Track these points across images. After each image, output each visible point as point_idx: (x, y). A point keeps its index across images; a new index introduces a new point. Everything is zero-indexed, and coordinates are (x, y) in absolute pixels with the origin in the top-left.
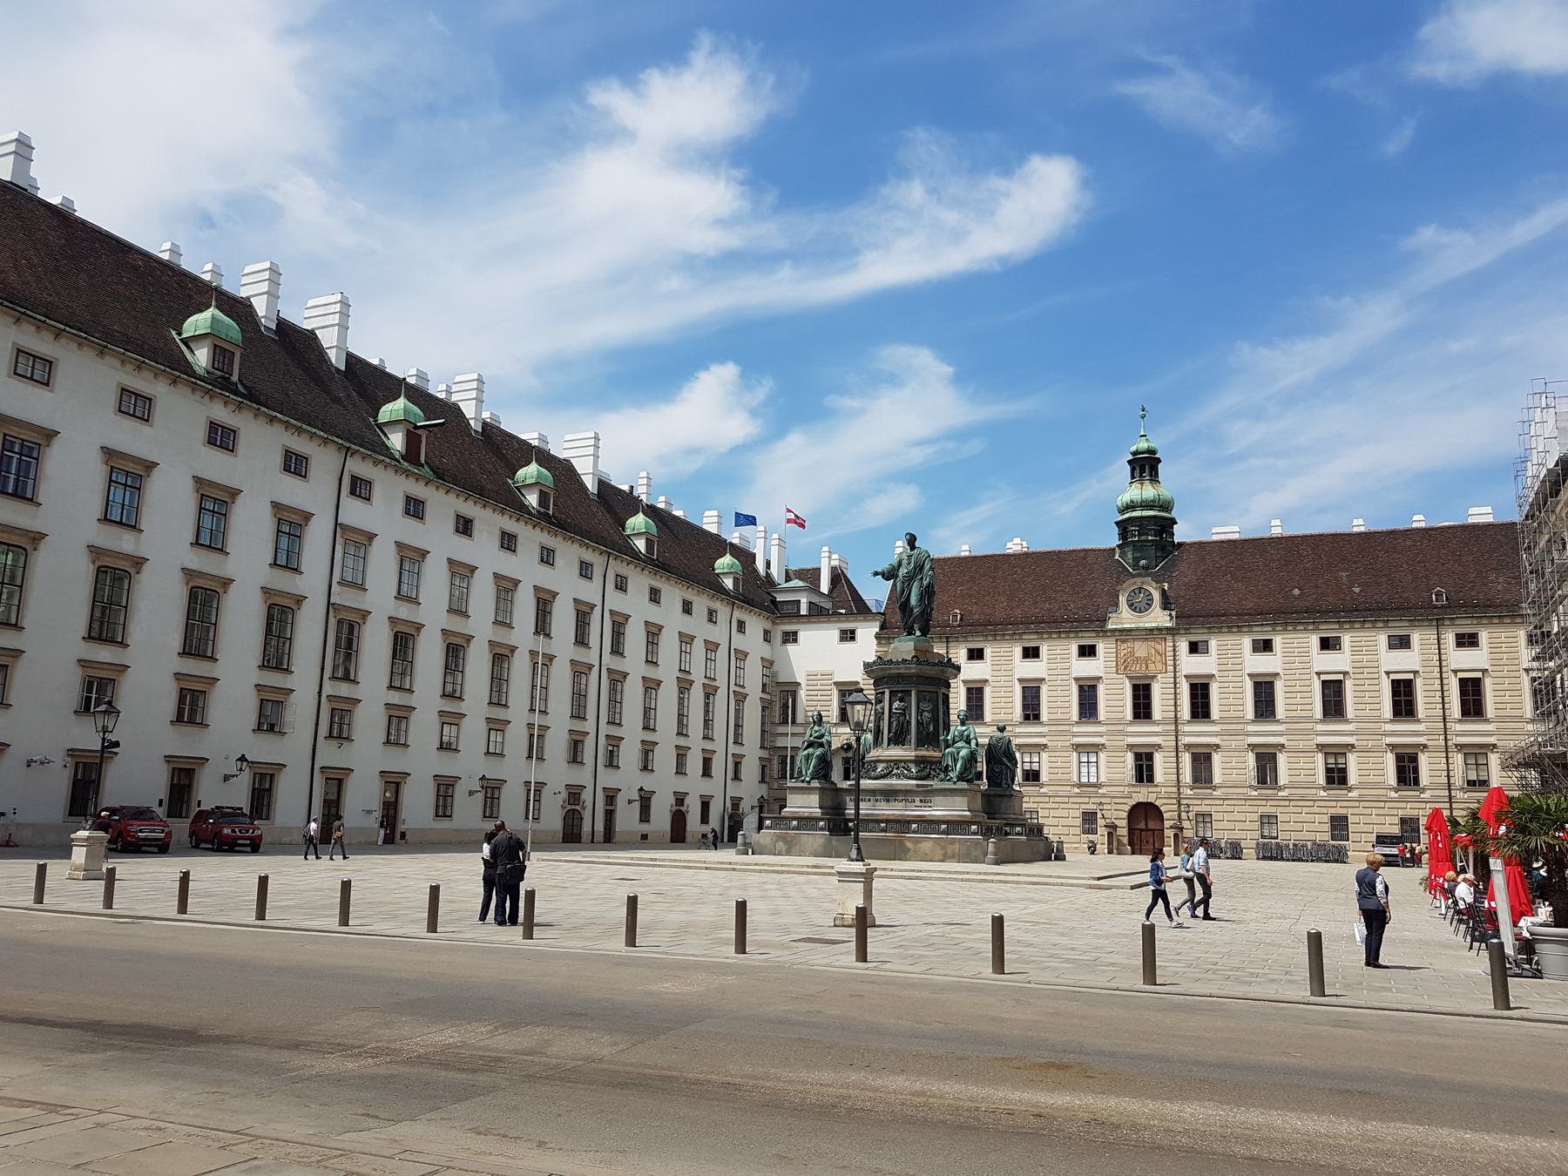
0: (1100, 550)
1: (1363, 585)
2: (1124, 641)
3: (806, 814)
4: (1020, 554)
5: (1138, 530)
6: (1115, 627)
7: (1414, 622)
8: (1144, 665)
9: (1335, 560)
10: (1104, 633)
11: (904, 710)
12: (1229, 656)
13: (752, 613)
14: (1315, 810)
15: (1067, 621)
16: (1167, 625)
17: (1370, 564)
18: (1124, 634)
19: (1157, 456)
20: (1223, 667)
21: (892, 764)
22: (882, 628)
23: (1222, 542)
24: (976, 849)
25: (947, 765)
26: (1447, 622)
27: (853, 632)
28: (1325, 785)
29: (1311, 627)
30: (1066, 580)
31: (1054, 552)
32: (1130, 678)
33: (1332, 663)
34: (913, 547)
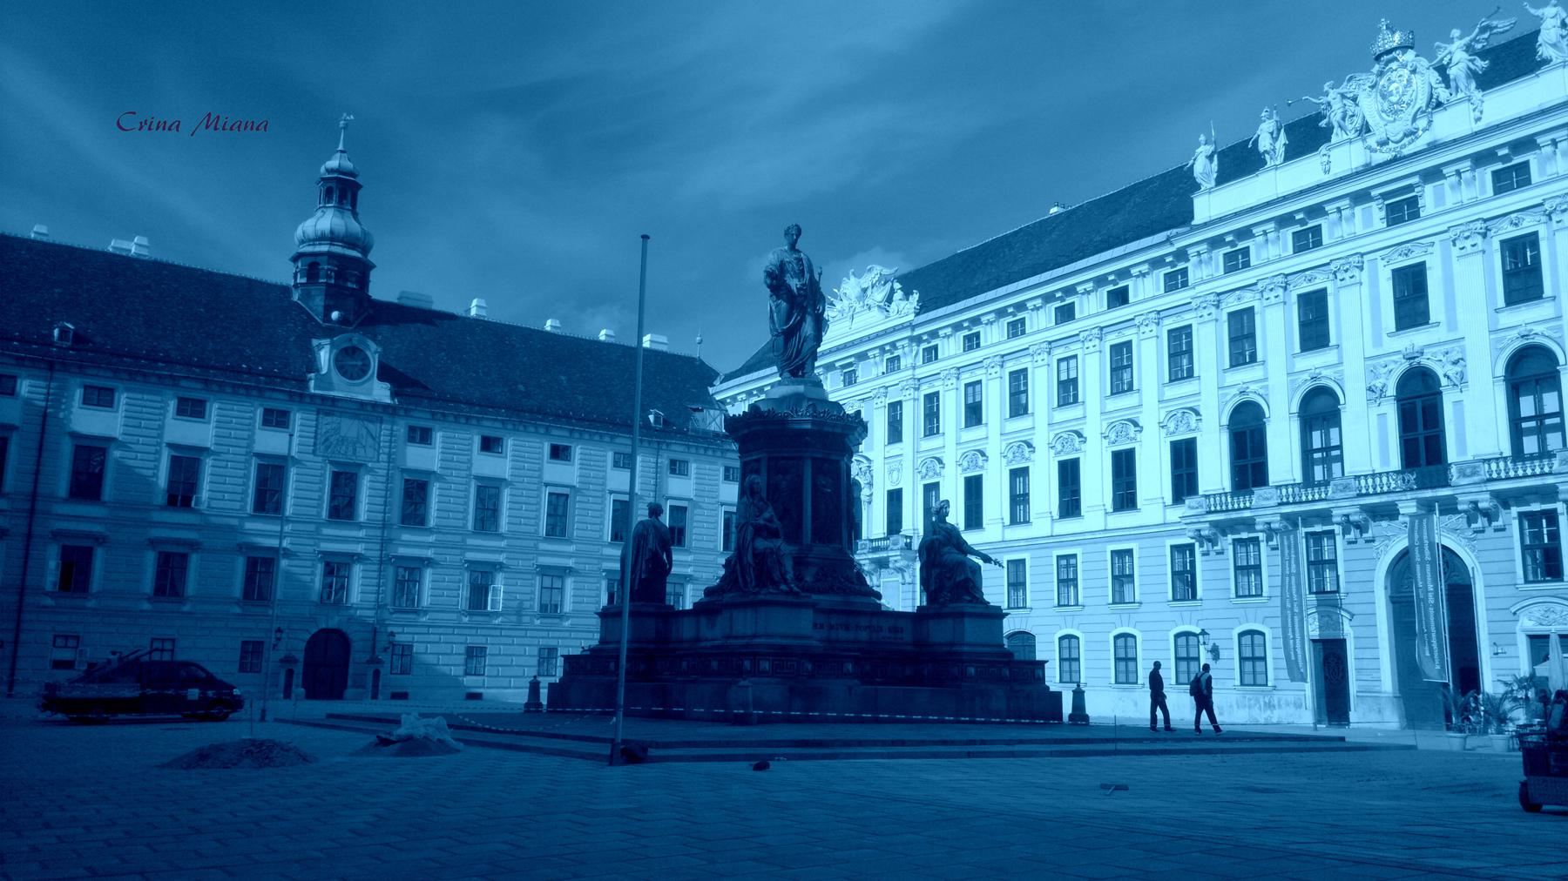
2: (328, 414)
5: (335, 271)
6: (317, 392)
8: (351, 448)
10: (302, 398)
14: (527, 641)
15: (249, 372)
16: (388, 401)
18: (328, 405)
19: (358, 180)
25: (967, 580)
26: (664, 447)
31: (202, 270)
32: (332, 463)
33: (564, 474)
34: (793, 247)
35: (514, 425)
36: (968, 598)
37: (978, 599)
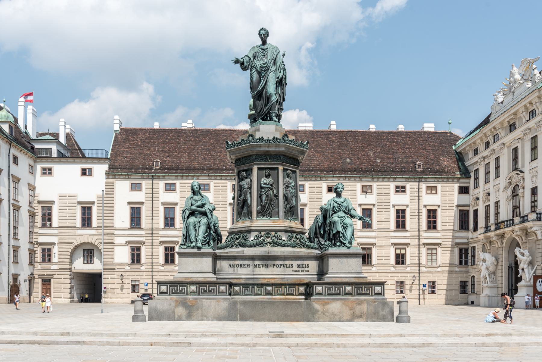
0: (239, 131)
1: (381, 158)
3: (200, 280)
4: (192, 130)
7: (407, 180)
9: (365, 145)
11: (271, 185)
12: (315, 193)
13: (22, 152)
17: (383, 147)
20: (311, 200)
21: (263, 233)
22: (110, 168)
23: (306, 131)
24: (383, 309)
25: (338, 232)
26: (423, 180)
27: (91, 170)
28: (395, 265)
29: (357, 179)
30: (221, 146)
31: (212, 130)
35: (343, 178)
36: (338, 244)
37: (344, 244)
